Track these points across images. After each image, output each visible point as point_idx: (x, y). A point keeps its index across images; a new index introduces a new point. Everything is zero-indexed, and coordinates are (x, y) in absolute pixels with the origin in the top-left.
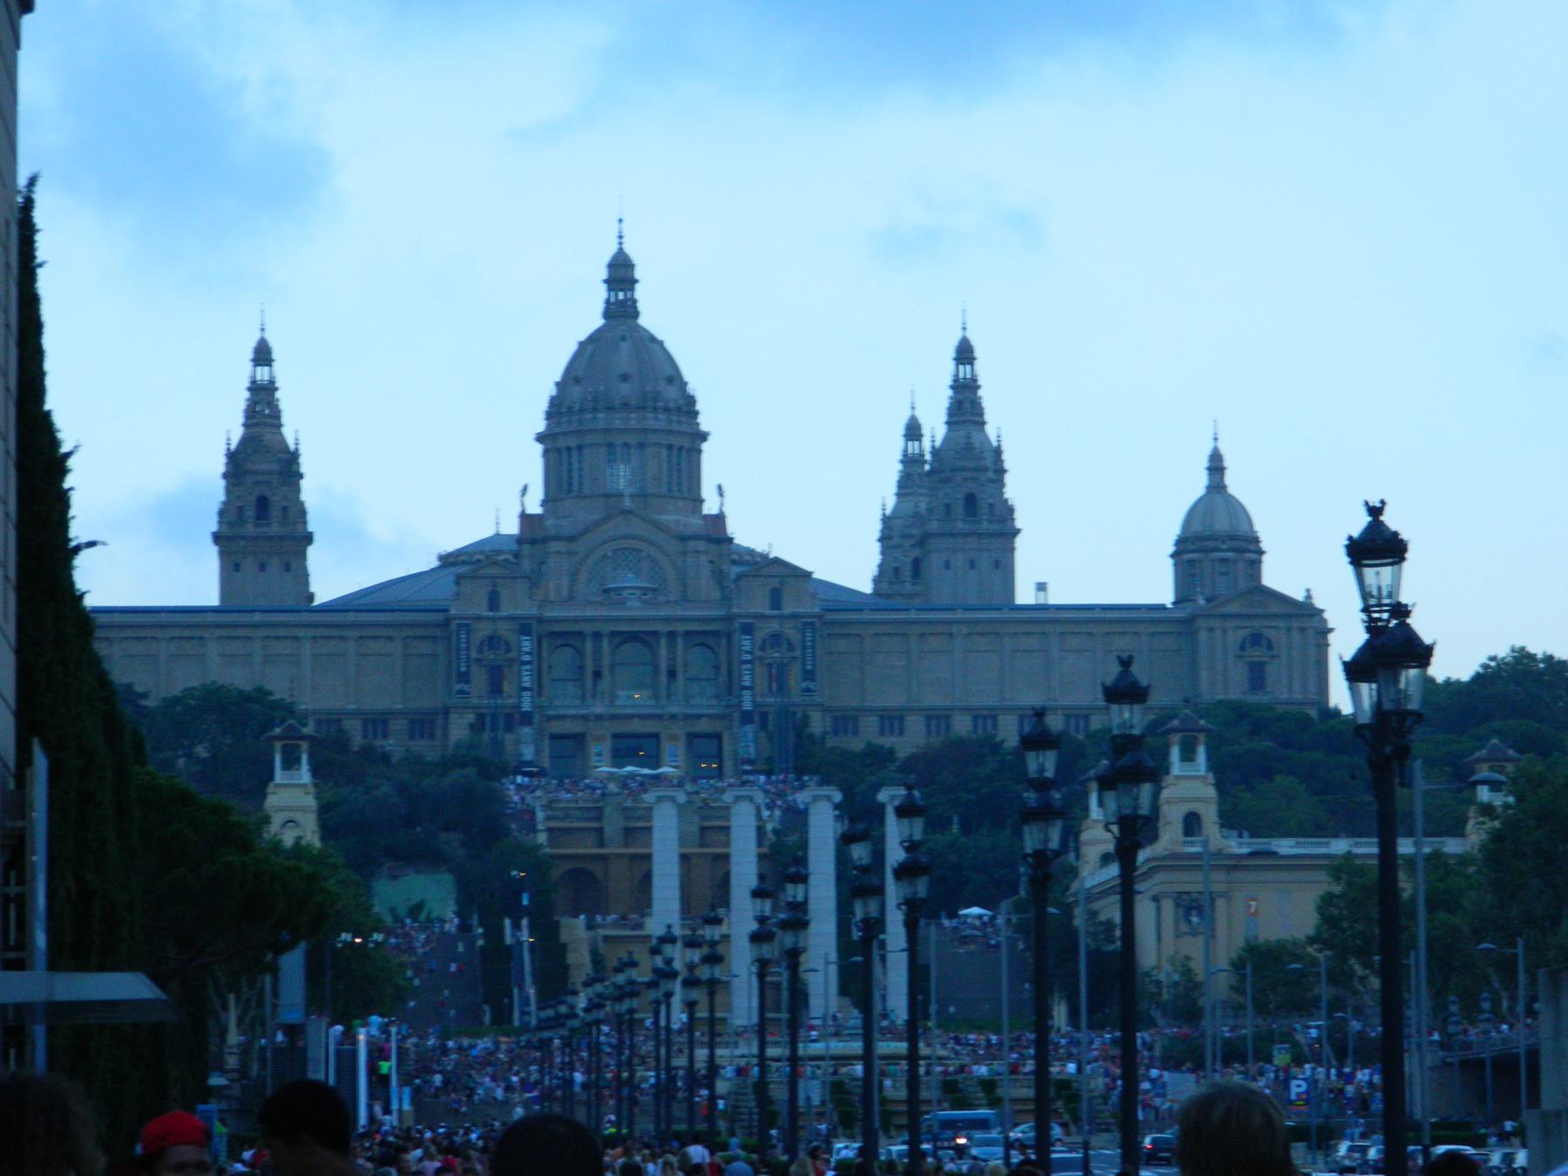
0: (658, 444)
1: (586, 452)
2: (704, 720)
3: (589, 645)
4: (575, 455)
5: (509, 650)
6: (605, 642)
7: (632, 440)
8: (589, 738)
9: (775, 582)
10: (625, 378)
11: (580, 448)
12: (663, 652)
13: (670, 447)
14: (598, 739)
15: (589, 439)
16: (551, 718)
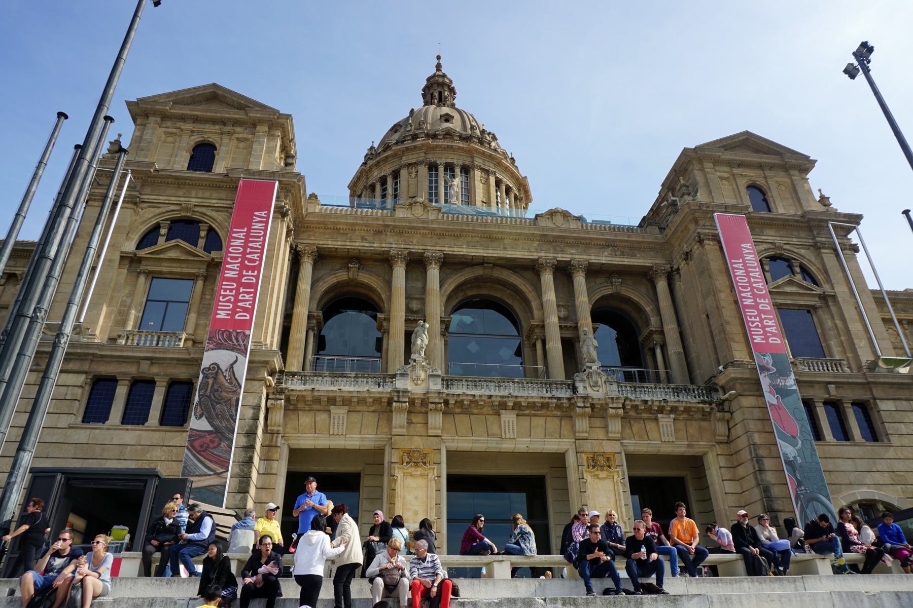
0: (487, 172)
1: (404, 173)
2: (666, 421)
3: (399, 272)
4: (390, 181)
5: (214, 241)
6: (434, 273)
7: (458, 160)
8: (392, 456)
9: (754, 175)
10: (447, 118)
11: (396, 175)
12: (550, 296)
13: (498, 183)
14: (416, 459)
15: (405, 160)
16: (293, 405)
